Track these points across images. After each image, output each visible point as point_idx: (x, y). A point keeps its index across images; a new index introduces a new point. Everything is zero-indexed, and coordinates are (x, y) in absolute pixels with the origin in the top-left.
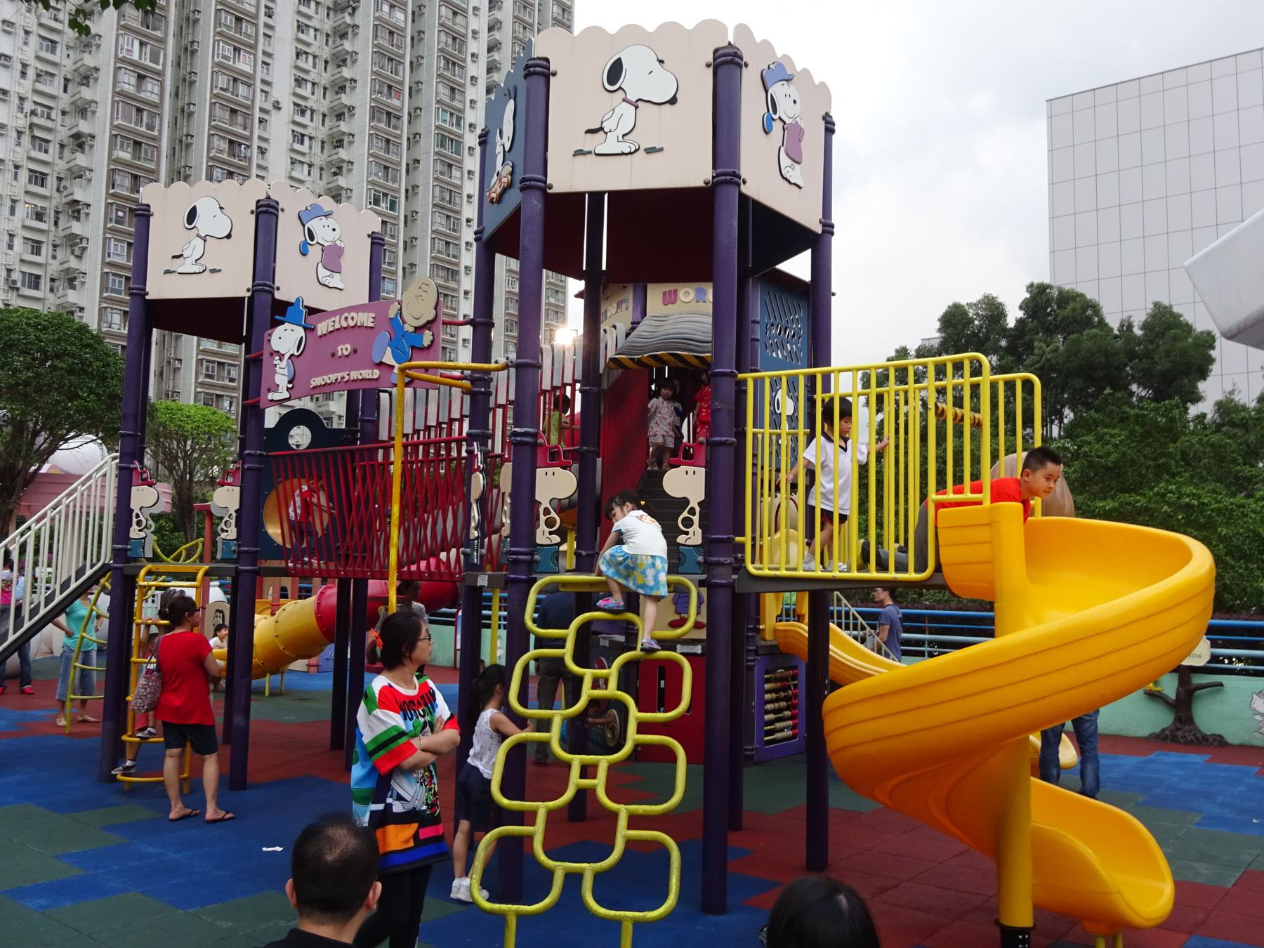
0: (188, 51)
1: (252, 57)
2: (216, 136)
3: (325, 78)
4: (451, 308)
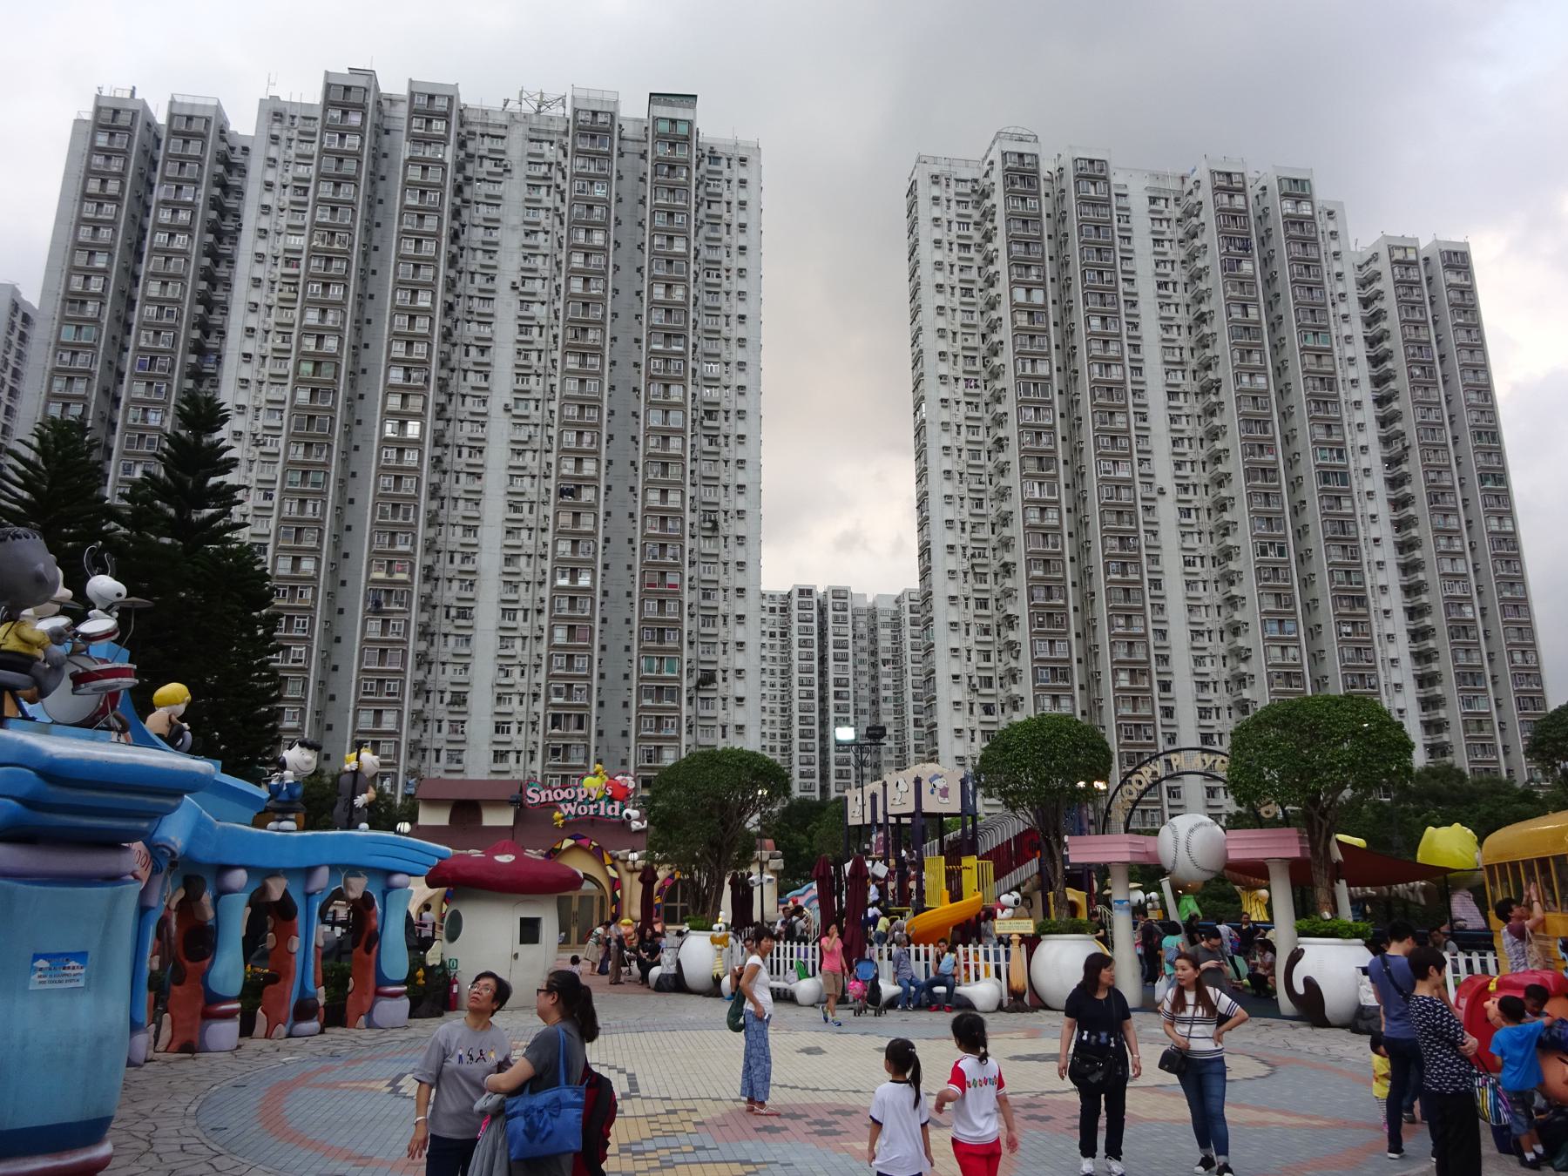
0: (1079, 474)
3: (1202, 454)
4: (1363, 634)
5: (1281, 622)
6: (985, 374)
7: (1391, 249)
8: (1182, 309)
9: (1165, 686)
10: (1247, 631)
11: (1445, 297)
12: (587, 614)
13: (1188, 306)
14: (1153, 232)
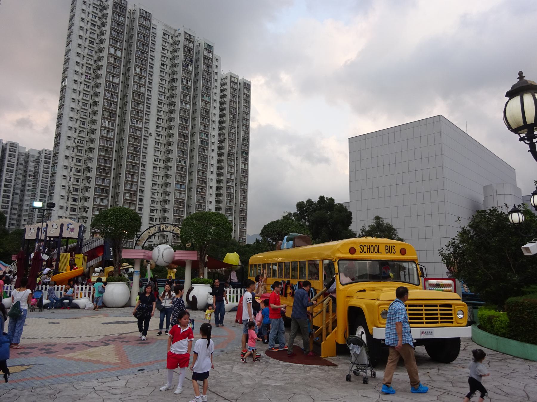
0: (123, 122)
3: (166, 125)
5: (181, 185)
6: (93, 76)
7: (231, 77)
8: (168, 75)
9: (141, 200)
10: (170, 186)
11: (243, 96)
13: (170, 74)
14: (163, 45)
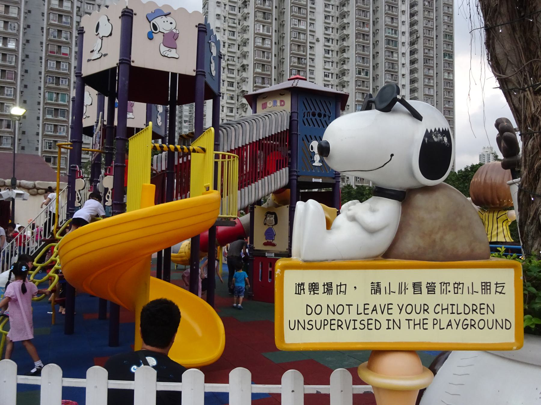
0: (282, 25)
1: (305, 22)
2: (293, 57)
3: (337, 25)
12: (13, 64)
